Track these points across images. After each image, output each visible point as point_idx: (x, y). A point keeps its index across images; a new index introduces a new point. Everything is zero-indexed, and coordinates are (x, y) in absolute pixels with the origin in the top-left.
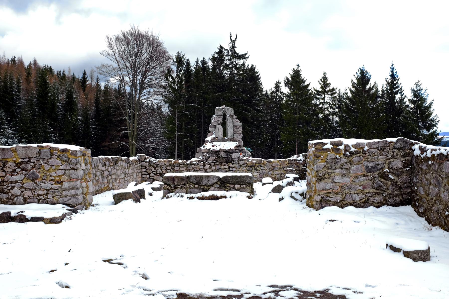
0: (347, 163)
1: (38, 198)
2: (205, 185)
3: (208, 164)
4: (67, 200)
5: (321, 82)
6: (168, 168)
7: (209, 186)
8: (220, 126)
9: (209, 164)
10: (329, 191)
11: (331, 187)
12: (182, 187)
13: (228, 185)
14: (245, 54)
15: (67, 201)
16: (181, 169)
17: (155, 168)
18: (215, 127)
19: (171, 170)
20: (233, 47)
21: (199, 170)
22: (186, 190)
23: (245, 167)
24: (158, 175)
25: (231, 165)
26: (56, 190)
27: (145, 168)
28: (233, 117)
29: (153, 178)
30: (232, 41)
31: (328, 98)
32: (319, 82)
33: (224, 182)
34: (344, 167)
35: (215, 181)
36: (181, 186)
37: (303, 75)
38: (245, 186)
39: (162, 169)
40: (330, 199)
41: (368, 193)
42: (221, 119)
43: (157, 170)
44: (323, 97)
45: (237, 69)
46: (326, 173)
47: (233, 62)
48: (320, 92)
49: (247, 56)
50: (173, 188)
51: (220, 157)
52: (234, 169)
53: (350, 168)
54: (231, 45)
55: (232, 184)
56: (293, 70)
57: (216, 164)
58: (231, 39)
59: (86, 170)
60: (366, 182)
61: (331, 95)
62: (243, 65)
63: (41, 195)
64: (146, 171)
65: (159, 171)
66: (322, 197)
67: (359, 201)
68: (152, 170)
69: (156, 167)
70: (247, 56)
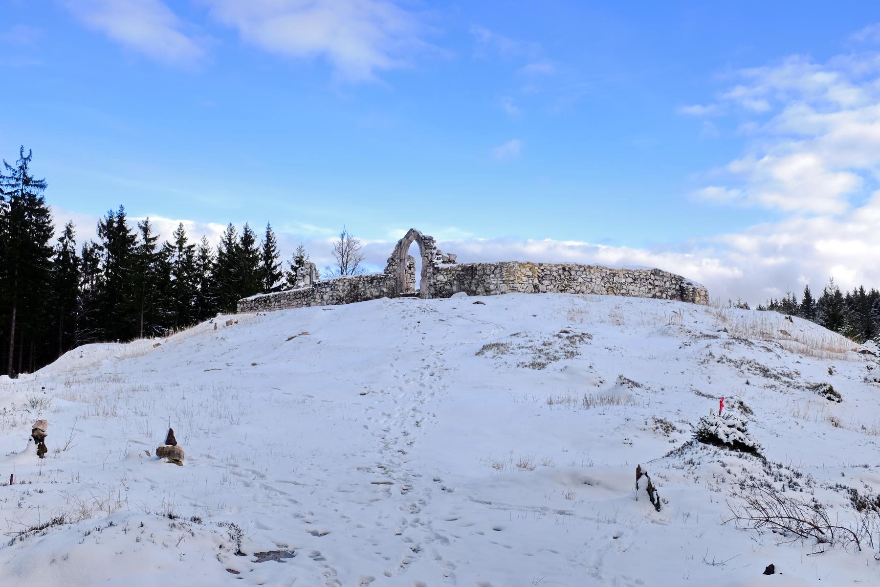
5: (176, 235)
30: (22, 158)
32: (174, 234)
48: (175, 248)
54: (20, 163)
56: (110, 211)
58: (21, 155)
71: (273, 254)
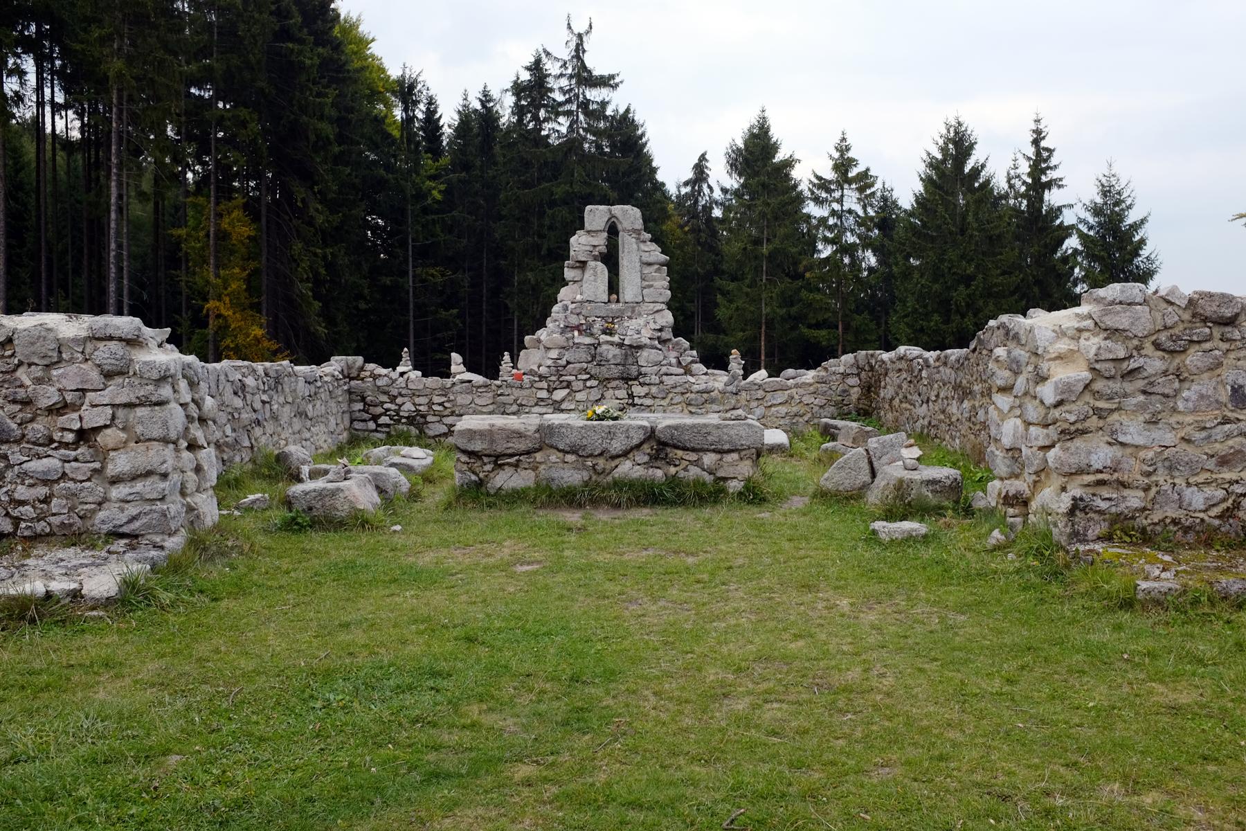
0: (1165, 373)
1: (15, 513)
2: (601, 454)
3: (565, 384)
4: (125, 520)
6: (437, 399)
7: (613, 458)
8: (599, 263)
9: (569, 385)
10: (1100, 476)
11: (1109, 461)
12: (518, 461)
13: (680, 453)
14: (612, 77)
15: (127, 523)
16: (478, 401)
17: (393, 399)
18: (582, 265)
19: (446, 405)
20: (579, 51)
21: (536, 404)
22: (533, 474)
23: (683, 394)
24: (403, 420)
25: (638, 390)
26: (81, 482)
27: (363, 399)
28: (639, 234)
29: (387, 430)
31: (851, 200)
33: (665, 444)
34: (1157, 389)
35: (635, 441)
36: (517, 457)
37: (776, 133)
38: (735, 456)
39: (417, 400)
40: (1104, 505)
41: (1237, 482)
42: (601, 240)
43: (400, 406)
44: (837, 194)
45: (588, 113)
46: (1091, 412)
47: (577, 96)
48: (830, 182)
49: (617, 80)
50: (488, 467)
51: (603, 363)
52: (648, 402)
53: (1177, 392)
55: (694, 450)
57: (588, 384)
58: (569, 27)
59: (192, 406)
60: (1230, 443)
61: (861, 190)
62: (604, 104)
63: (22, 503)
64: (363, 410)
65: (408, 406)
66: (1074, 499)
67: (1204, 511)
68: (386, 406)
69: (395, 397)
70: (617, 80)
71: (1052, 175)
